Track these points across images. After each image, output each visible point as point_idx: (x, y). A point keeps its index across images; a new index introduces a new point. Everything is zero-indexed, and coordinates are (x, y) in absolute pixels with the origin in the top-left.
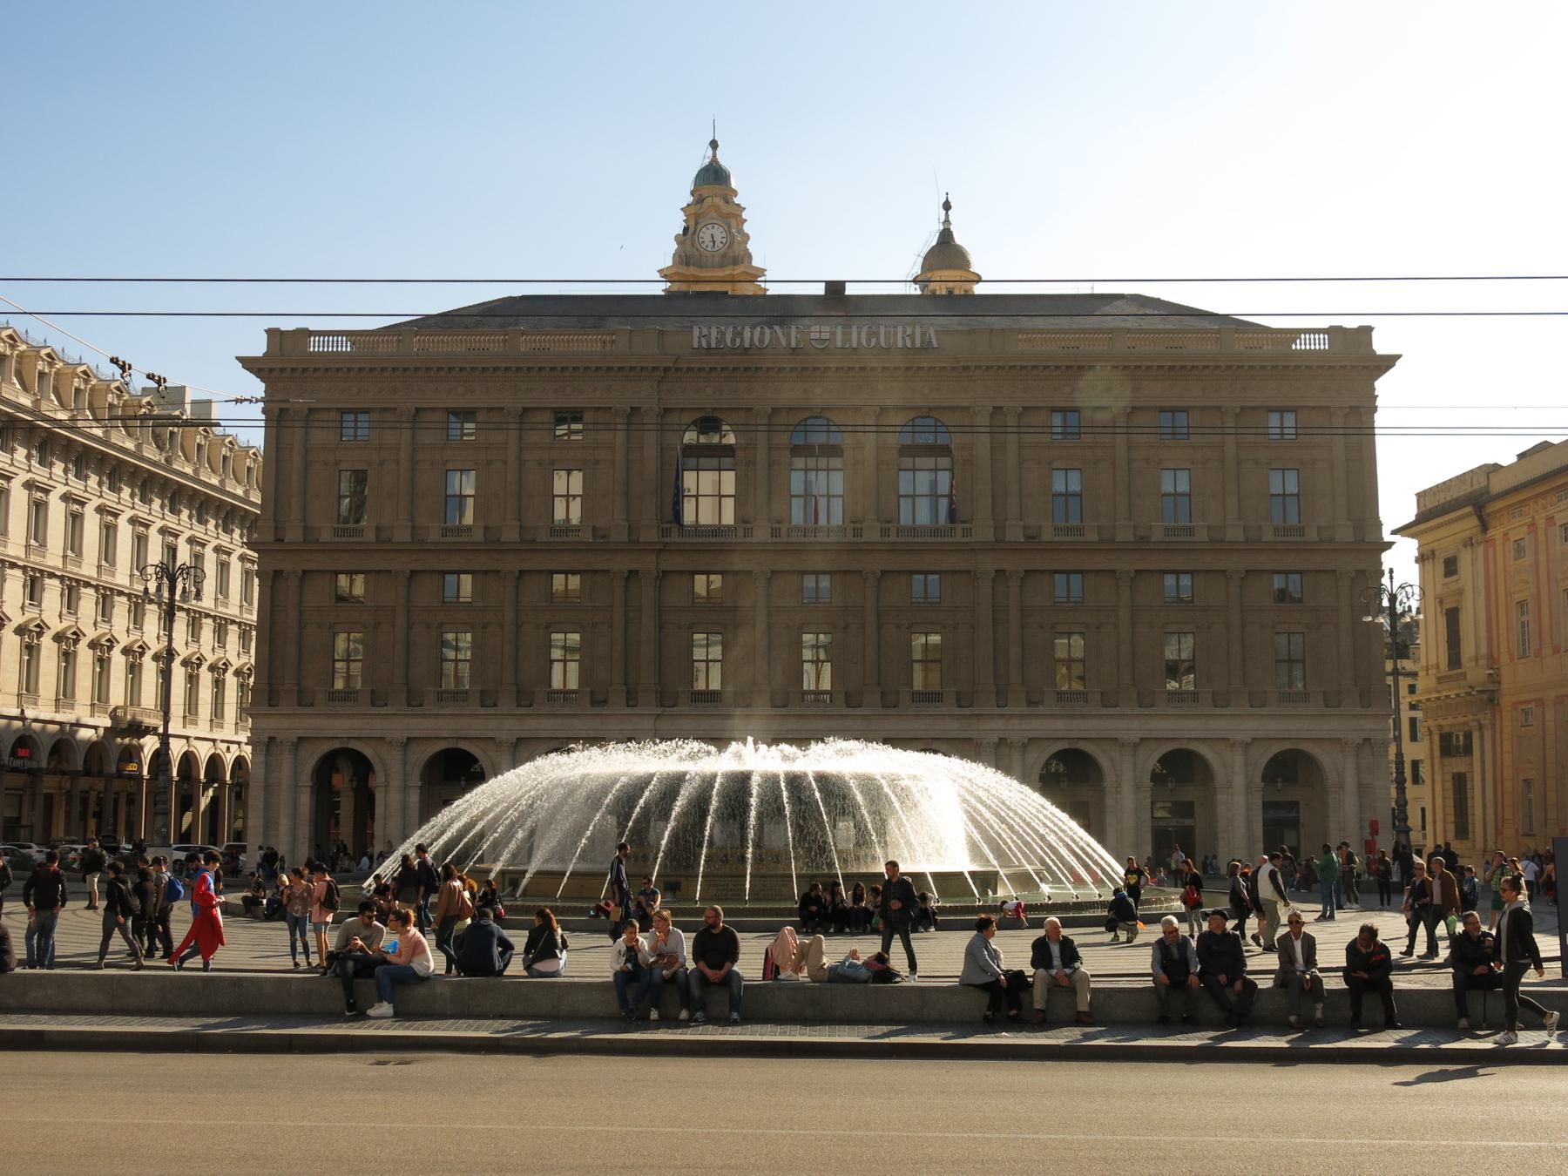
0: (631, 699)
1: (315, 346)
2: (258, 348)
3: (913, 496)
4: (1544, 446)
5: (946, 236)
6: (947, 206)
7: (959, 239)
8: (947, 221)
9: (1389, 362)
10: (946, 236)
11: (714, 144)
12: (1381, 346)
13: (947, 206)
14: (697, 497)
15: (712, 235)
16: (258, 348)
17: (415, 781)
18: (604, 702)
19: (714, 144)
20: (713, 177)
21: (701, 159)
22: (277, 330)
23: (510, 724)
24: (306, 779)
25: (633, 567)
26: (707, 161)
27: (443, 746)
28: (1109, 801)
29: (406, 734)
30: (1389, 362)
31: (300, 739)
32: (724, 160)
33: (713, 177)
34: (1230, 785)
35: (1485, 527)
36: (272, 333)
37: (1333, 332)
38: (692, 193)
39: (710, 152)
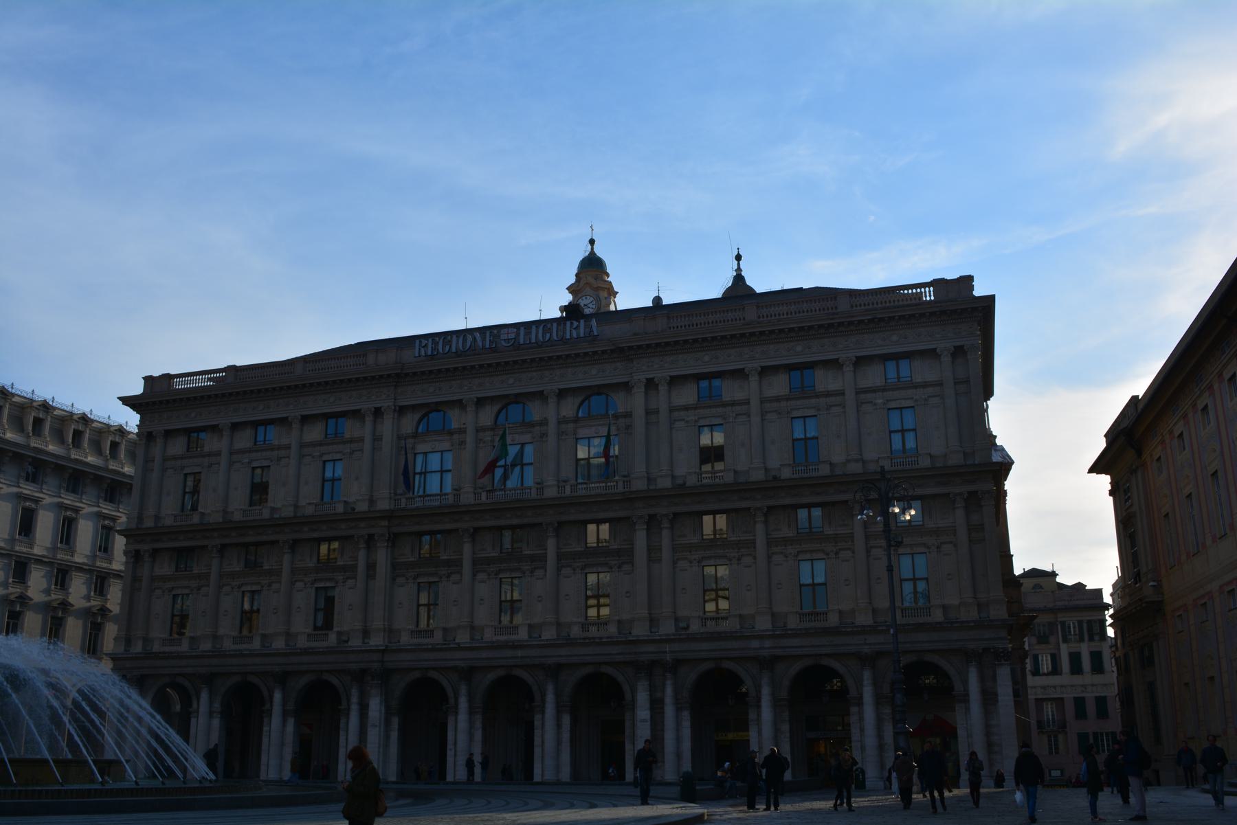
1: (178, 385)
5: (739, 279)
6: (738, 258)
7: (750, 282)
8: (739, 269)
10: (739, 279)
12: (978, 291)
13: (738, 258)
16: (137, 389)
19: (592, 242)
20: (592, 267)
21: (584, 251)
22: (151, 377)
28: (752, 716)
32: (599, 252)
34: (861, 697)
35: (1139, 453)
36: (148, 380)
37: (938, 284)
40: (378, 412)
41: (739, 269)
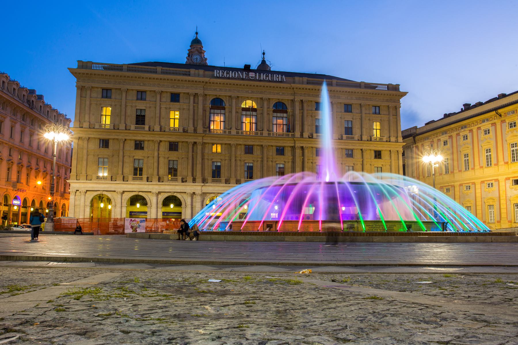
0: (194, 180)
2: (75, 66)
3: (276, 124)
4: (433, 121)
5: (264, 62)
6: (264, 54)
7: (268, 63)
8: (264, 58)
9: (405, 94)
10: (264, 62)
11: (197, 33)
13: (264, 54)
14: (214, 121)
15: (196, 58)
17: (125, 204)
18: (186, 181)
19: (197, 33)
20: (196, 42)
21: (192, 37)
23: (156, 187)
24: (88, 203)
25: (195, 141)
26: (195, 38)
27: (134, 194)
29: (123, 190)
30: (405, 94)
31: (87, 191)
33: (196, 42)
38: (190, 46)
39: (196, 35)
40: (196, 95)
41: (264, 58)
